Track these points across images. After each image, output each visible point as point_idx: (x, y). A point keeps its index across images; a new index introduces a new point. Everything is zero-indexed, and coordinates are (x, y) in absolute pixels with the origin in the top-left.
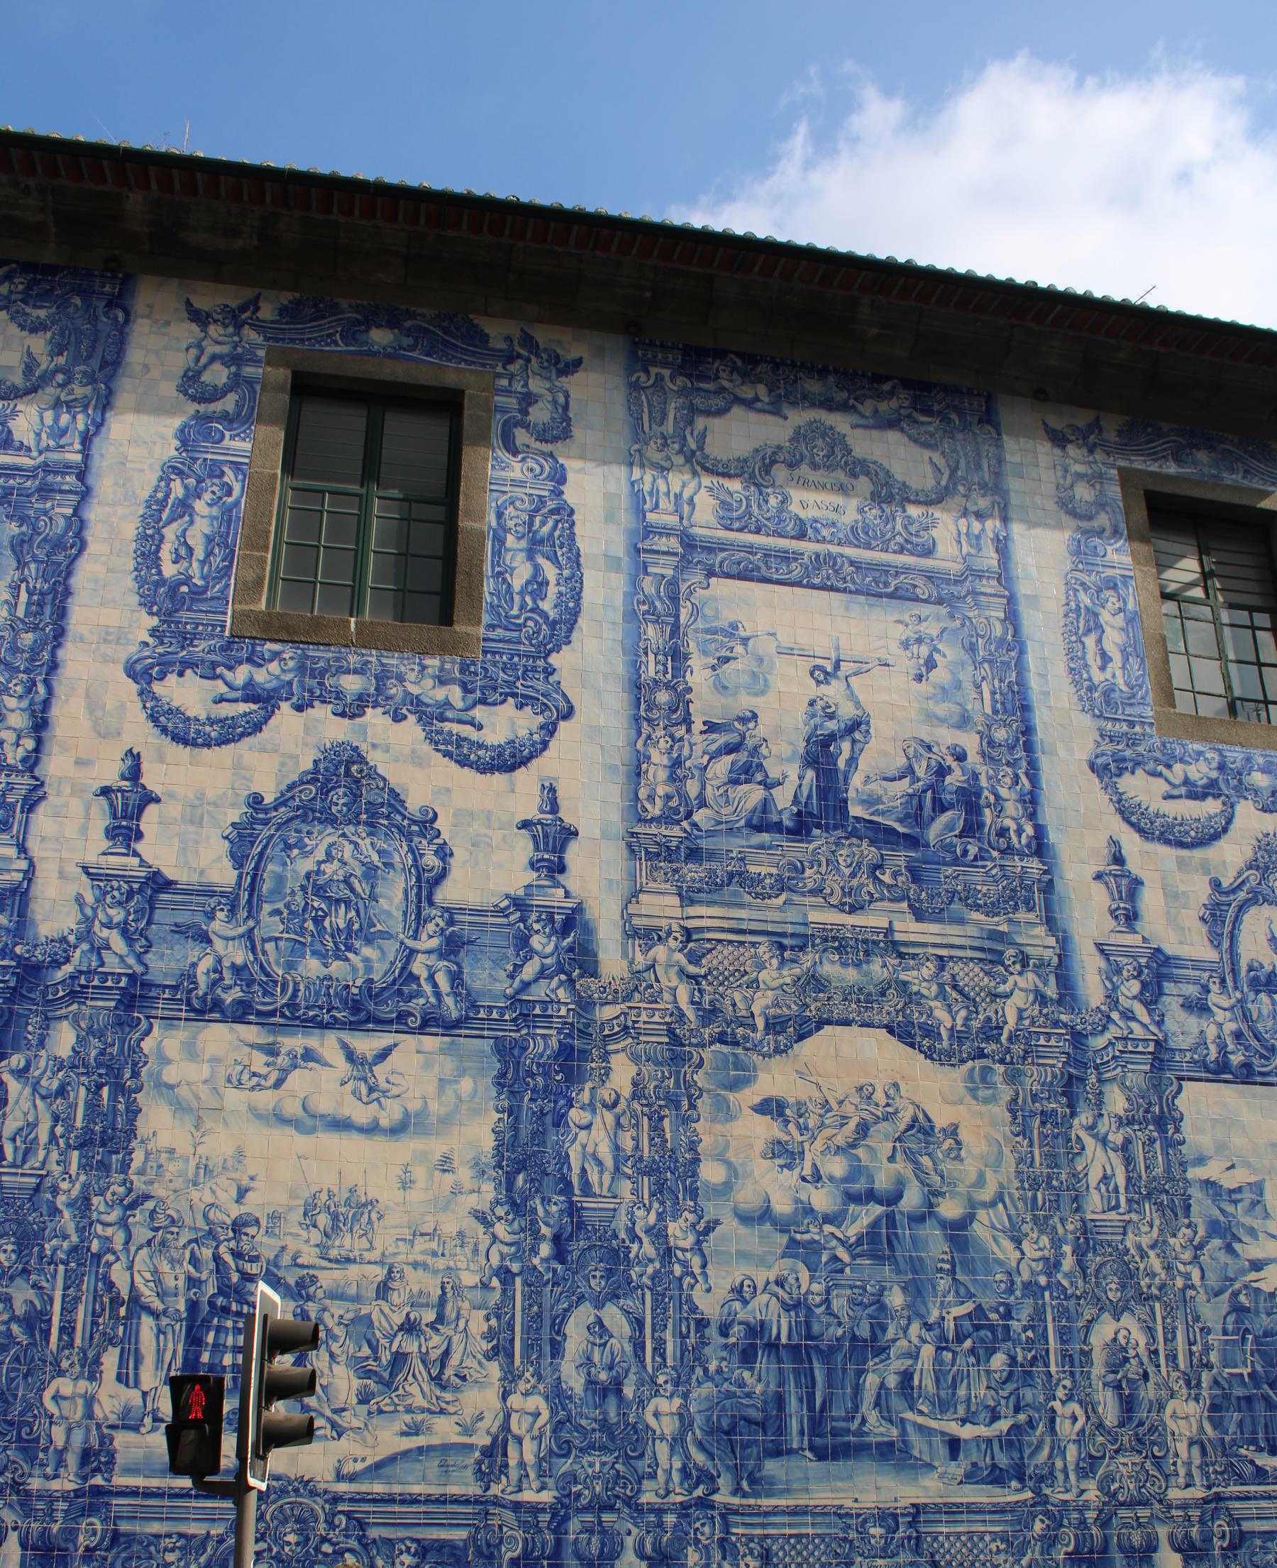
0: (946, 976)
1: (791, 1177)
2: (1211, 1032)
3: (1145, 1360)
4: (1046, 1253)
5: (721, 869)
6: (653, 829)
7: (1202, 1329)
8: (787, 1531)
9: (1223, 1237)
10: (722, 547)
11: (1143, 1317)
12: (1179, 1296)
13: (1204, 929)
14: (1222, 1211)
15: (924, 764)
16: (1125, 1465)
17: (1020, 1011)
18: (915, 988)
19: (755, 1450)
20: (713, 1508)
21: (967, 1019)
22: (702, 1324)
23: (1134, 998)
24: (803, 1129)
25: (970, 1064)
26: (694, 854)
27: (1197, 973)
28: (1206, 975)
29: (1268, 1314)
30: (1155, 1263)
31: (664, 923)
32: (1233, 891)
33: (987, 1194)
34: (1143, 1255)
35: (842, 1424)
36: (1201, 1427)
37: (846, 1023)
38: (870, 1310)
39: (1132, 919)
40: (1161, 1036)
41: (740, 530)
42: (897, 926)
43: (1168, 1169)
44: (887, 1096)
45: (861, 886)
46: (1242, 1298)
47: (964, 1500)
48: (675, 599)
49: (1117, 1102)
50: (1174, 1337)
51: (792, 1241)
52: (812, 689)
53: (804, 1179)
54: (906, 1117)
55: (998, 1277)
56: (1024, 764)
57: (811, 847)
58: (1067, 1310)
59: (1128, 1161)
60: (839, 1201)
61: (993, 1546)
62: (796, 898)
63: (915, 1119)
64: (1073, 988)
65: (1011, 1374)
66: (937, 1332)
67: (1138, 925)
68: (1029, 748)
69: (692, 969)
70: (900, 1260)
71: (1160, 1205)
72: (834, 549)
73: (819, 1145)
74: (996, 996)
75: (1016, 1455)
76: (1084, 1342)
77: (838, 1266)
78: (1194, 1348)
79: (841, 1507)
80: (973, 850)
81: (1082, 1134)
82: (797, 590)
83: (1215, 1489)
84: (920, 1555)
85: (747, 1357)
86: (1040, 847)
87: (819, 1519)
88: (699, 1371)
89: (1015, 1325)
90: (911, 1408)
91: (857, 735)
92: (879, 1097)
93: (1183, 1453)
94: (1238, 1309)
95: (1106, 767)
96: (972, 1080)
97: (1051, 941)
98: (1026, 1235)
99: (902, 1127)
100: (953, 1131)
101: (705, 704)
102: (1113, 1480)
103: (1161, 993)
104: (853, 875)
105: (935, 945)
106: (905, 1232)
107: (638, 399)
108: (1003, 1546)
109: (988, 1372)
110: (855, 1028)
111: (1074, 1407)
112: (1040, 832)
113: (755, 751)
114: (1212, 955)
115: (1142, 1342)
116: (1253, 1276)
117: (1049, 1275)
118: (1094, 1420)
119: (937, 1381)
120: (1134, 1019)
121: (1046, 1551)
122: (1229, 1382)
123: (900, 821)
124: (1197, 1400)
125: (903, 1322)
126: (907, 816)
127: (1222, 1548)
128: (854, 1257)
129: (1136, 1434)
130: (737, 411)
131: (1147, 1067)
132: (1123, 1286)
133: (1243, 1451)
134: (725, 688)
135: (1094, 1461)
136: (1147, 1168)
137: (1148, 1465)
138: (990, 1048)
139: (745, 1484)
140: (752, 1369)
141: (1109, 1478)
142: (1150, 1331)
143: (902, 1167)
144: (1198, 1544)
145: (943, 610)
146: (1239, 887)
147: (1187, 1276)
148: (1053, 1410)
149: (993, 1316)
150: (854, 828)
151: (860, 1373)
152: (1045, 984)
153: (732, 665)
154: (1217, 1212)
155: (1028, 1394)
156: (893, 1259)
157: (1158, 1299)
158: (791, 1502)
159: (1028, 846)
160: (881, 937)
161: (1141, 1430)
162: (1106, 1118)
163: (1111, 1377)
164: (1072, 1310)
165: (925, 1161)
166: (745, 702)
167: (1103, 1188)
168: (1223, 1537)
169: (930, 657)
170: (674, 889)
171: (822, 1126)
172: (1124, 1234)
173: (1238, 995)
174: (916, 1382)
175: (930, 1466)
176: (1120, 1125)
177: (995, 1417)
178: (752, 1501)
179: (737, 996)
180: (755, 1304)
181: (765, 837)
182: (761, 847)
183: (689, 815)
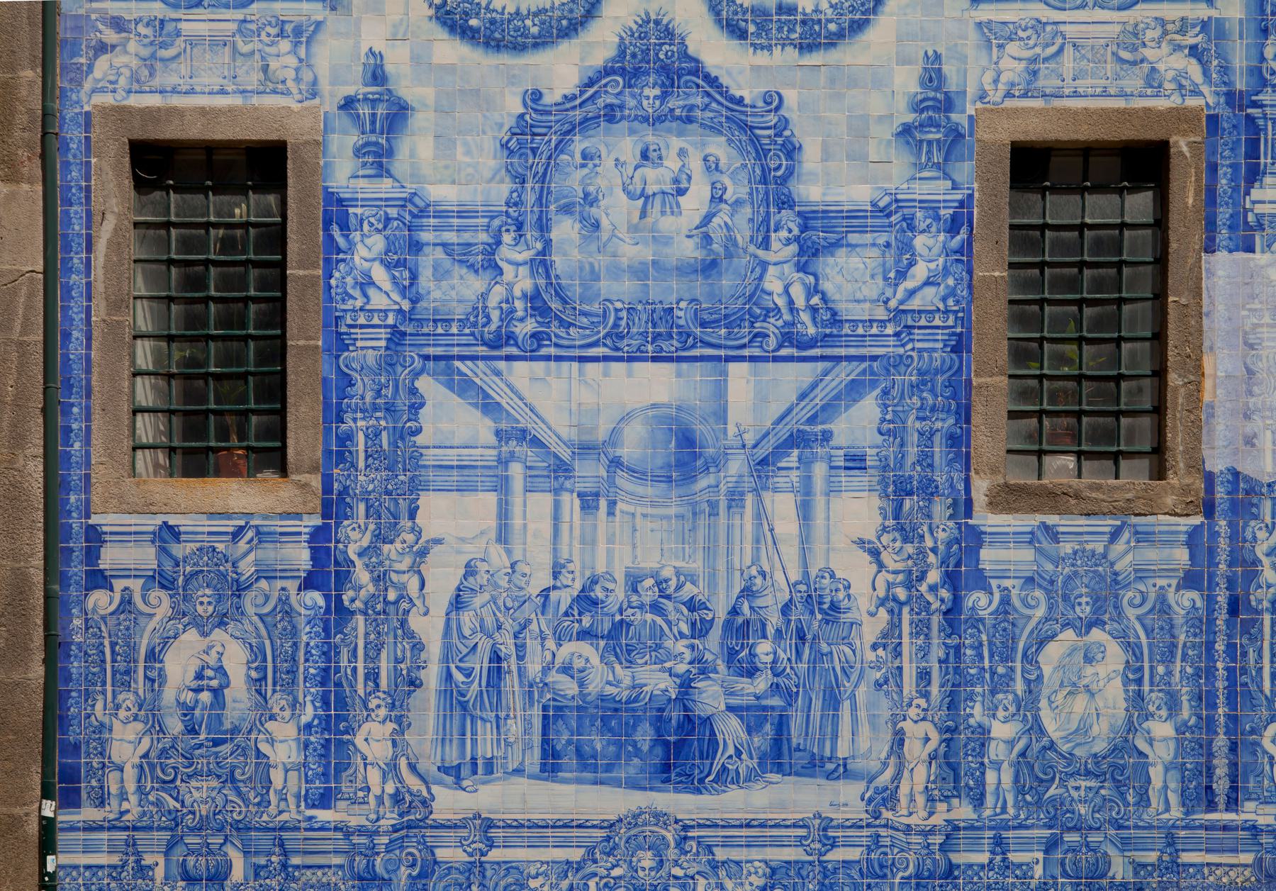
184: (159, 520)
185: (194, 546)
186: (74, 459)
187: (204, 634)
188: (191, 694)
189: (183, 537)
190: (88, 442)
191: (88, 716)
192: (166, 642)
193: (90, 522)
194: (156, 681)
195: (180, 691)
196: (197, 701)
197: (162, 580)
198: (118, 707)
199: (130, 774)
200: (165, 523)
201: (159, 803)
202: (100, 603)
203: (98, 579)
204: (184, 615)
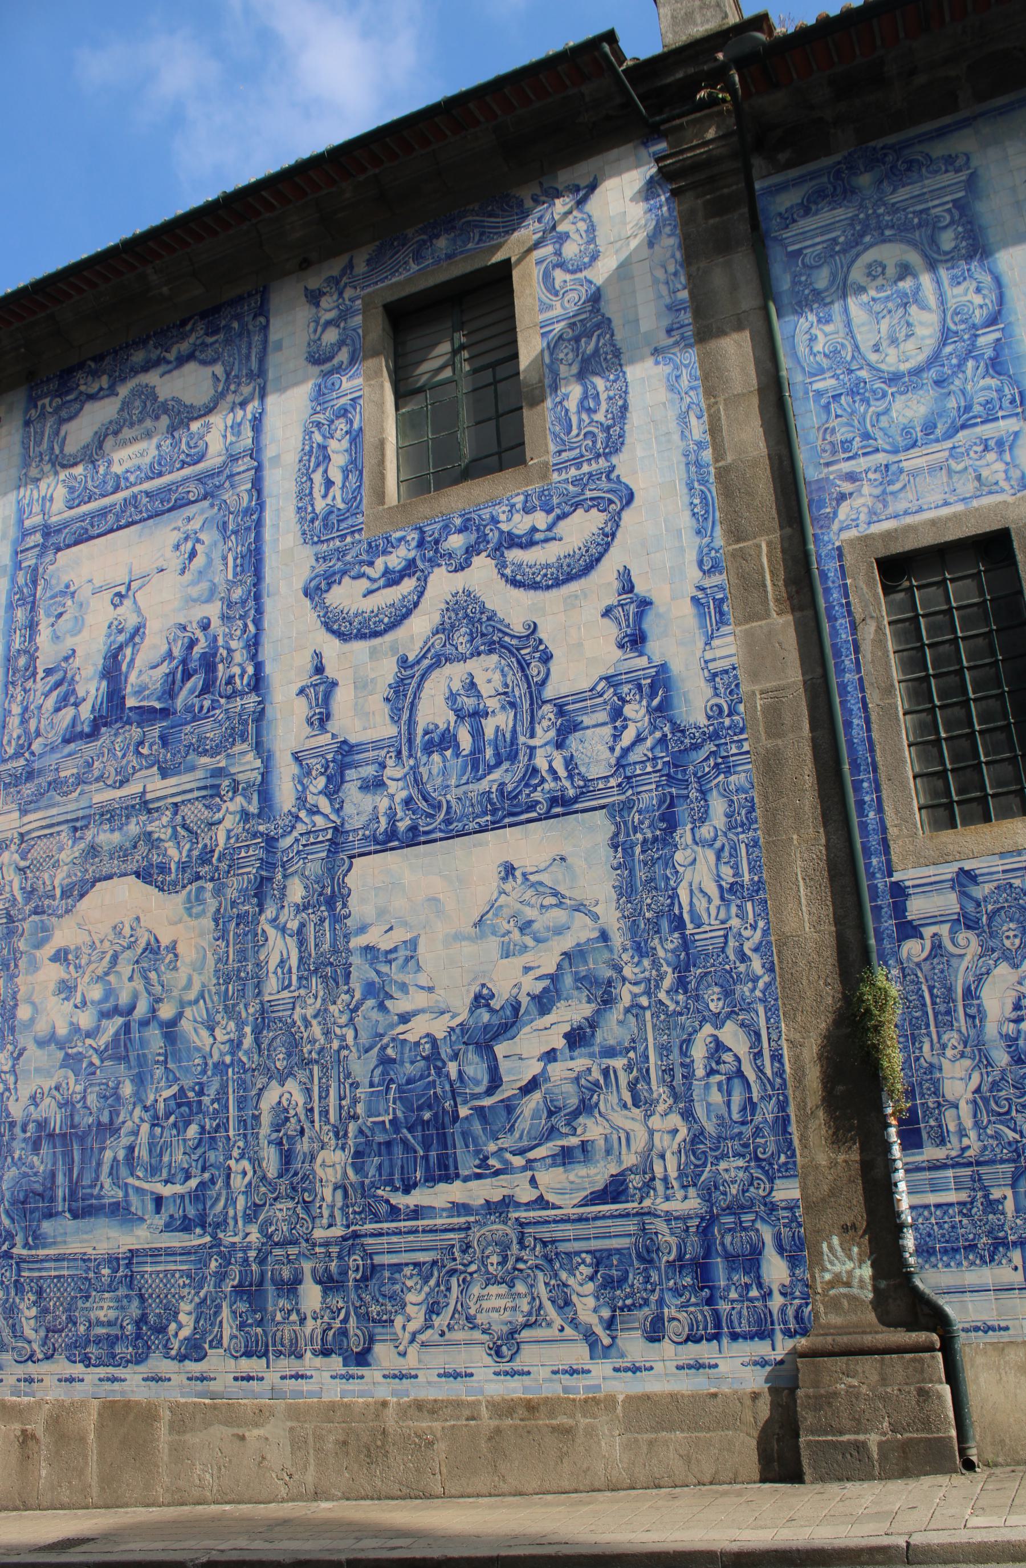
0: (179, 818)
1: (68, 1006)
2: (384, 804)
3: (303, 1117)
4: (232, 1035)
5: (43, 781)
6: (9, 765)
7: (351, 1085)
8: (53, 1273)
9: (376, 996)
10: (65, 524)
11: (303, 1080)
12: (335, 1057)
13: (386, 708)
14: (378, 972)
15: (180, 643)
16: (281, 1210)
17: (229, 831)
18: (156, 836)
19: (36, 1215)
20: (12, 1258)
21: (190, 850)
22: (12, 1125)
23: (320, 793)
24: (78, 967)
25: (189, 886)
26: (30, 775)
27: (376, 753)
28: (383, 753)
29: (412, 1063)
30: (317, 1030)
31: (9, 835)
32: (418, 662)
33: (192, 995)
34: (307, 1024)
35: (89, 1191)
36: (345, 1173)
37: (109, 877)
38: (110, 1101)
39: (321, 720)
40: (338, 822)
41: (79, 505)
42: (148, 789)
43: (334, 944)
44: (132, 929)
45: (129, 762)
46: (390, 1052)
47: (163, 1245)
48: (35, 582)
49: (296, 892)
50: (327, 1095)
51: (67, 1054)
52: (110, 613)
53: (76, 1007)
54: (142, 943)
55: (197, 1061)
56: (253, 612)
57: (99, 743)
58: (244, 1082)
59: (302, 943)
60: (96, 1019)
61: (181, 1281)
62: (87, 788)
63: (148, 944)
64: (270, 800)
65: (201, 1140)
66: (152, 1112)
67: (330, 726)
68: (258, 598)
69: (23, 864)
70: (132, 1058)
71: (324, 978)
72: (136, 489)
73: (87, 979)
74: (212, 824)
75: (200, 1207)
76: (256, 1108)
77: (93, 1069)
78: (344, 1103)
79: (85, 1254)
80: (207, 704)
81: (268, 929)
82: (109, 536)
83: (353, 1228)
84: (132, 1289)
85: (36, 1146)
86: (258, 683)
87: (72, 1264)
88: (9, 1159)
89: (206, 1100)
90: (132, 1175)
91: (137, 639)
92: (127, 931)
93: (329, 1198)
94: (385, 1061)
95: (318, 588)
96: (189, 900)
97: (258, 763)
98: (218, 1023)
99: (139, 951)
100: (173, 948)
101: (47, 652)
102: (271, 1224)
103: (343, 782)
104: (124, 756)
105: (173, 795)
106: (135, 1035)
107: (29, 432)
108: (187, 1282)
109: (184, 1140)
110: (115, 879)
111: (245, 1164)
112: (259, 667)
113: (72, 679)
114: (391, 730)
115: (301, 1103)
116: (401, 1028)
117: (233, 1054)
118: (259, 1173)
119: (150, 1151)
120: (318, 812)
121: (218, 1285)
122: (372, 1130)
123: (159, 699)
124: (343, 1149)
125: (131, 1107)
126: (164, 692)
127: (356, 1280)
128: (102, 1061)
129: (292, 1183)
130: (88, 407)
131: (324, 854)
132: (289, 1055)
133: (380, 1192)
134: (58, 638)
135: (257, 1207)
136: (316, 945)
137: (299, 1210)
138: (203, 870)
139: (30, 1239)
140: (38, 1155)
141: (268, 1222)
142: (308, 1091)
143: (138, 984)
144: (336, 1277)
145: (206, 504)
146: (424, 657)
147: (343, 1039)
148: (229, 1168)
149: (191, 1094)
150: (129, 717)
151: (103, 1149)
152: (249, 803)
153: (65, 617)
154: (373, 975)
155: (212, 1156)
156: (126, 1059)
157: (317, 1062)
158: (57, 1252)
159: (249, 685)
160: (138, 800)
161: (295, 1180)
162: (286, 909)
163: (274, 1135)
164: (249, 1082)
165: (153, 975)
166: (70, 642)
167: (279, 970)
168: (357, 1270)
169: (194, 548)
170: (16, 807)
171: (89, 963)
172: (293, 1009)
173: (412, 762)
174: (136, 1154)
175: (142, 1219)
176: (298, 911)
177: (188, 1177)
178: (33, 1252)
179: (46, 876)
180: (43, 1106)
181: (72, 746)
182: (70, 755)
183: (30, 745)
184: (955, 867)
185: (992, 886)
186: (870, 827)
187: (1016, 966)
188: (1011, 1025)
189: (980, 879)
190: (880, 810)
191: (917, 1059)
192: (980, 979)
193: (893, 879)
194: (976, 1017)
195: (1001, 1024)
196: (1019, 1031)
197: (967, 921)
198: (944, 1047)
199: (965, 1110)
200: (961, 869)
201: (997, 1136)
202: (913, 952)
203: (909, 930)
204: (993, 951)
